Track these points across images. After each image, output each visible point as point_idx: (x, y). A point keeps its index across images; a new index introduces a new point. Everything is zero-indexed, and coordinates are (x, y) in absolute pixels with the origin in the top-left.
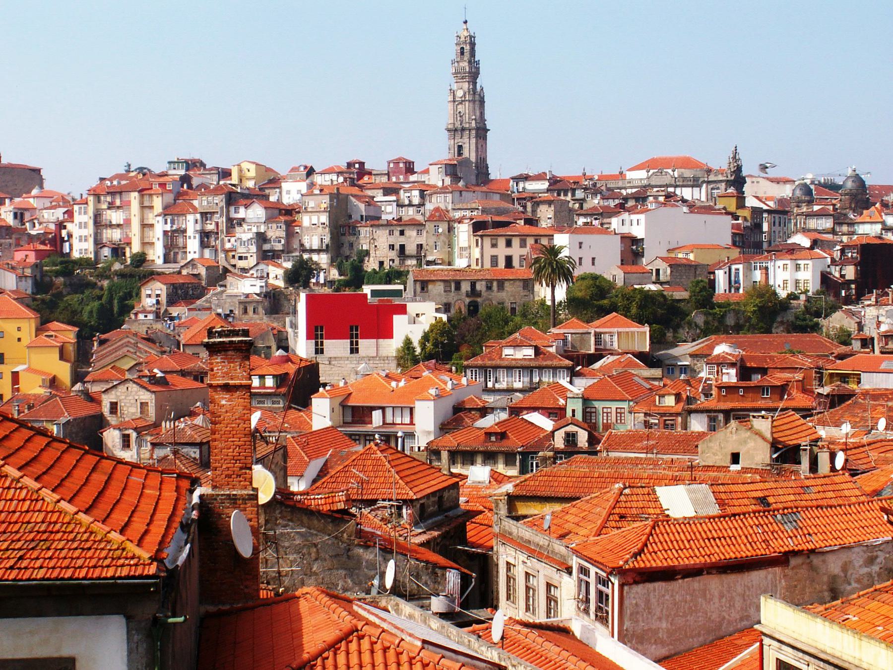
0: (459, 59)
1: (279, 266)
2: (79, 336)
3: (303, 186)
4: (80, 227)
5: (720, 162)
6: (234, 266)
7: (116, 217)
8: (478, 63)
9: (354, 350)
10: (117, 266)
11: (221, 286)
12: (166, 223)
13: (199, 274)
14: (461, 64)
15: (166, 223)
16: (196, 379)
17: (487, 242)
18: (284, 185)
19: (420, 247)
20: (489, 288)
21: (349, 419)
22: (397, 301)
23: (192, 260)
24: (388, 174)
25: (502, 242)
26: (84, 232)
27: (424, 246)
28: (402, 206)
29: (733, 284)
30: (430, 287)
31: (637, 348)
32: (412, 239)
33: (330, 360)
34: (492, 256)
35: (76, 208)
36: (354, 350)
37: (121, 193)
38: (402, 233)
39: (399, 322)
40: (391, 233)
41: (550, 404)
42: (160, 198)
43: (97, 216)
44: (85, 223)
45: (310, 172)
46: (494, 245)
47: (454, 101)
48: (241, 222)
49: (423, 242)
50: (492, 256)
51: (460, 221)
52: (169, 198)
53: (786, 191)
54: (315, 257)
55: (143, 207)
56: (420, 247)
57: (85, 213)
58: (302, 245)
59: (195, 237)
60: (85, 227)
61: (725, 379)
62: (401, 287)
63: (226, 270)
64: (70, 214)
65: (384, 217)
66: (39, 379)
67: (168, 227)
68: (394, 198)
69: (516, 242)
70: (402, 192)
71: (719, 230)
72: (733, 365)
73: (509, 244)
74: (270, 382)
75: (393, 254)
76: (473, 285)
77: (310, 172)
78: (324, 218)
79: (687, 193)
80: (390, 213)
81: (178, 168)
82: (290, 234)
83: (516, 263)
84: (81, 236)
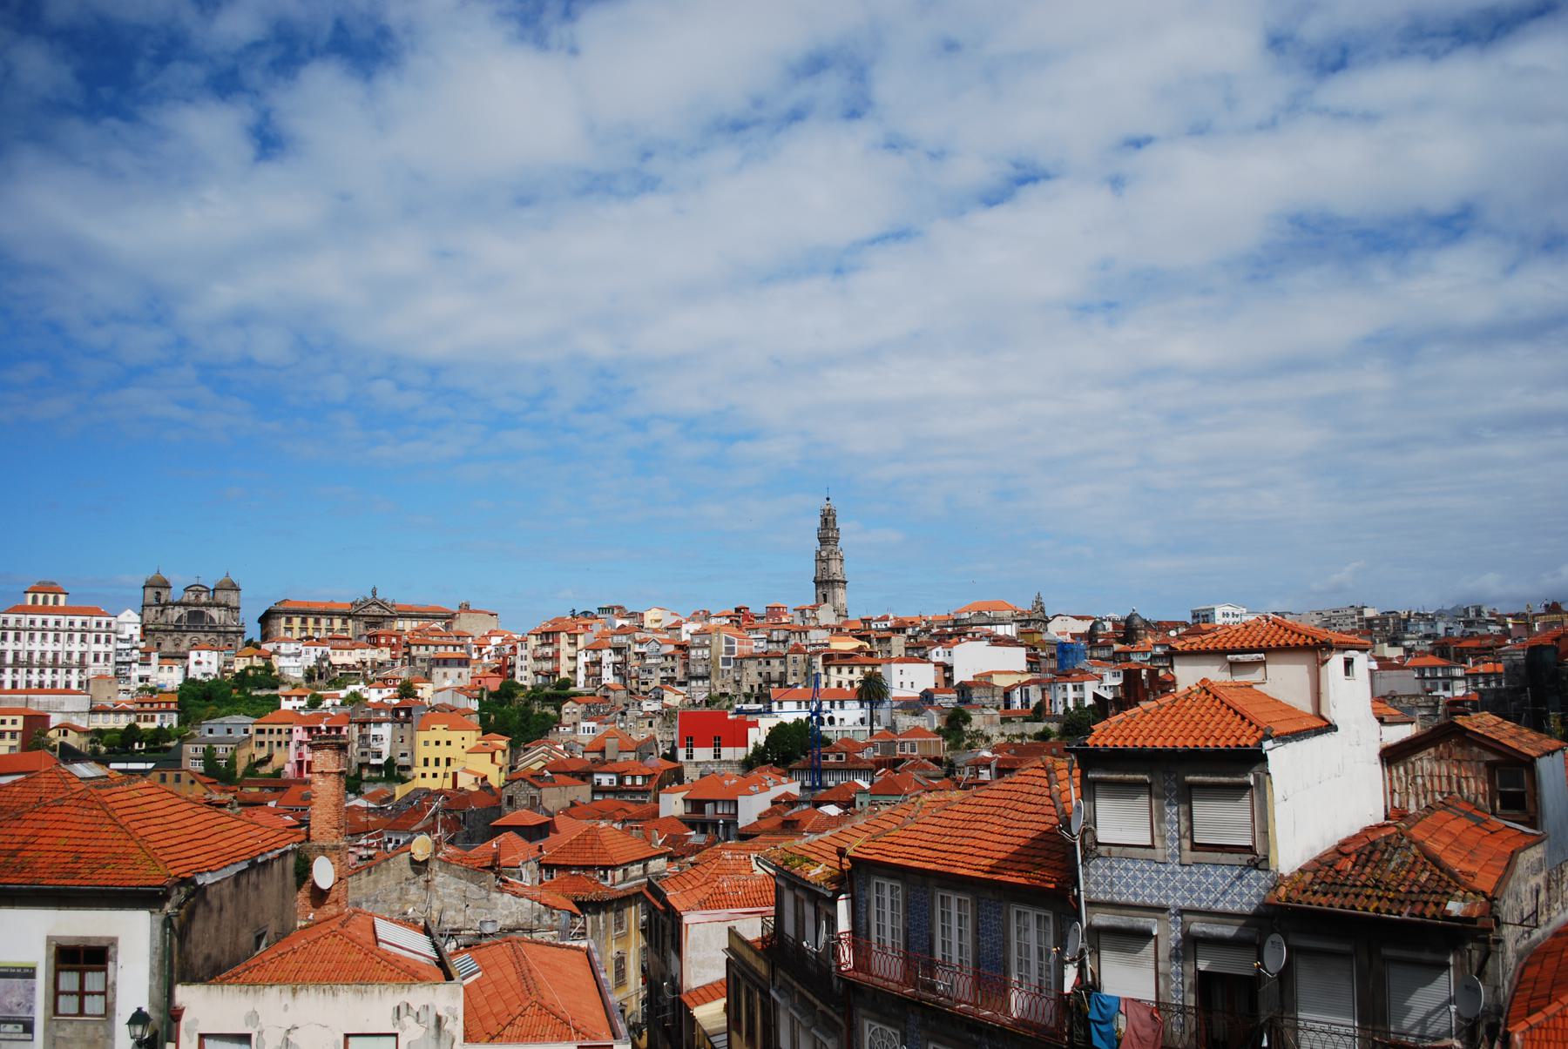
2: (511, 744)
5: (1025, 605)
7: (549, 650)
9: (717, 756)
10: (547, 690)
16: (583, 779)
17: (833, 670)
18: (684, 627)
21: (689, 809)
22: (749, 718)
25: (845, 670)
26: (524, 663)
29: (1025, 703)
31: (933, 754)
33: (697, 764)
36: (717, 756)
39: (752, 732)
41: (845, 798)
45: (707, 616)
46: (839, 671)
48: (643, 654)
53: (1084, 627)
61: (982, 778)
64: (514, 648)
66: (471, 778)
69: (857, 670)
71: (1016, 658)
72: (988, 767)
74: (639, 781)
75: (760, 680)
77: (707, 616)
79: (1001, 630)
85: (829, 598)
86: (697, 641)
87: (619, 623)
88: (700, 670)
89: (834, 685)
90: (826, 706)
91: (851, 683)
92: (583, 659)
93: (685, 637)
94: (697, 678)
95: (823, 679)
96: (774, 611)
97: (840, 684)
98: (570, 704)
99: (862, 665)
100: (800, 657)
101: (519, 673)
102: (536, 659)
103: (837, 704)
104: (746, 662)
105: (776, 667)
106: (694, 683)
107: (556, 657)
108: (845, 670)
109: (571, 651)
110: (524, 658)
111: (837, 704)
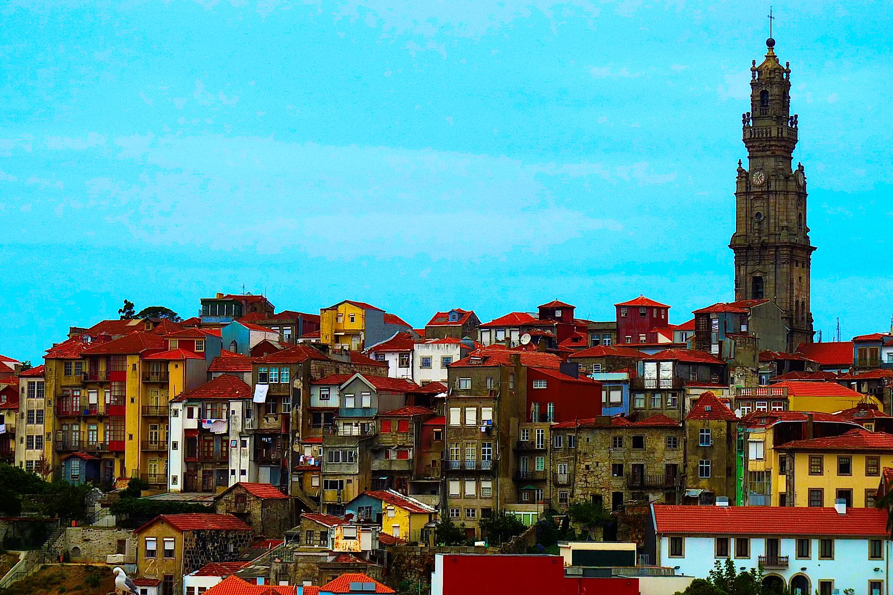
0: (757, 114)
1: (401, 504)
3: (455, 353)
4: (30, 421)
6: (317, 500)
8: (794, 120)
11: (289, 537)
12: (190, 416)
13: (249, 514)
14: (759, 123)
15: (190, 416)
17: (801, 465)
18: (420, 351)
19: (671, 469)
20: (803, 553)
23: (237, 485)
24: (617, 331)
25: (831, 464)
26: (38, 429)
27: (681, 467)
28: (643, 391)
30: (690, 544)
32: (658, 455)
34: (812, 491)
35: (24, 383)
37: (107, 357)
38: (638, 443)
40: (618, 443)
42: (181, 368)
43: (60, 400)
44: (40, 412)
46: (816, 470)
47: (747, 193)
48: (332, 415)
49: (679, 462)
50: (812, 491)
51: (750, 422)
52: (198, 366)
54: (471, 488)
55: (147, 383)
56: (671, 469)
57: (41, 394)
58: (446, 464)
59: (244, 444)
60: (39, 421)
62: (631, 547)
63: (299, 505)
65: (605, 412)
67: (193, 424)
68: (624, 376)
69: (858, 465)
70: (640, 363)
73: (844, 469)
75: (618, 484)
76: (773, 546)
78: (487, 414)
80: (616, 405)
81: (221, 313)
82: (423, 444)
83: (859, 501)
84: (30, 438)
85: (769, 289)
86: (466, 384)
87: (256, 337)
88: (470, 455)
89: (802, 500)
90: (788, 548)
91: (845, 495)
92: (179, 425)
93: (437, 374)
94: (463, 474)
95: (779, 484)
96: (642, 317)
97: (816, 495)
98: (156, 530)
99: (873, 455)
100: (717, 428)
101: (25, 456)
102: (62, 415)
103: (815, 546)
104: (584, 435)
105: (660, 454)
106: (454, 488)
107: (116, 413)
108: (831, 464)
109: (157, 399)
110: (36, 417)
111: (815, 546)
